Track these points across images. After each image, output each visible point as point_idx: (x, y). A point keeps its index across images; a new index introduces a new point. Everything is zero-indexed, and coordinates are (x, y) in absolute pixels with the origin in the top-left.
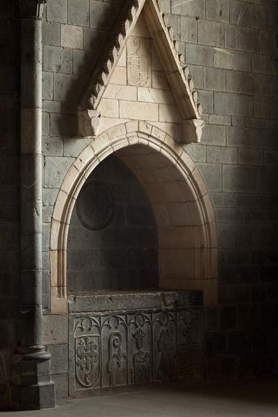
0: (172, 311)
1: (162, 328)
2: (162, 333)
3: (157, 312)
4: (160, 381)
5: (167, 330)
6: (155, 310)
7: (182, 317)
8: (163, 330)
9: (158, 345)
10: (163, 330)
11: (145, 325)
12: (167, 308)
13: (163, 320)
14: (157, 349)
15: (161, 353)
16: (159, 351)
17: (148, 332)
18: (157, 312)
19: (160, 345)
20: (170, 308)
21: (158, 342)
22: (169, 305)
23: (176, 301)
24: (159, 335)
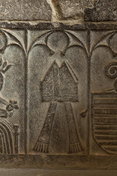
0: (77, 29)
1: (51, 60)
2: (51, 69)
3: (37, 28)
4: (44, 155)
5: (64, 65)
6: (32, 23)
7: (105, 42)
8: (55, 63)
9: (41, 89)
10: (55, 63)
11: (7, 50)
12: (64, 22)
13: (55, 43)
14: (38, 97)
15: (47, 105)
16: (43, 101)
17: (17, 65)
18: (37, 28)
19: (46, 91)
20: (71, 22)
21: (41, 84)
22: (70, 18)
23: (88, 12)
24: (45, 71)
